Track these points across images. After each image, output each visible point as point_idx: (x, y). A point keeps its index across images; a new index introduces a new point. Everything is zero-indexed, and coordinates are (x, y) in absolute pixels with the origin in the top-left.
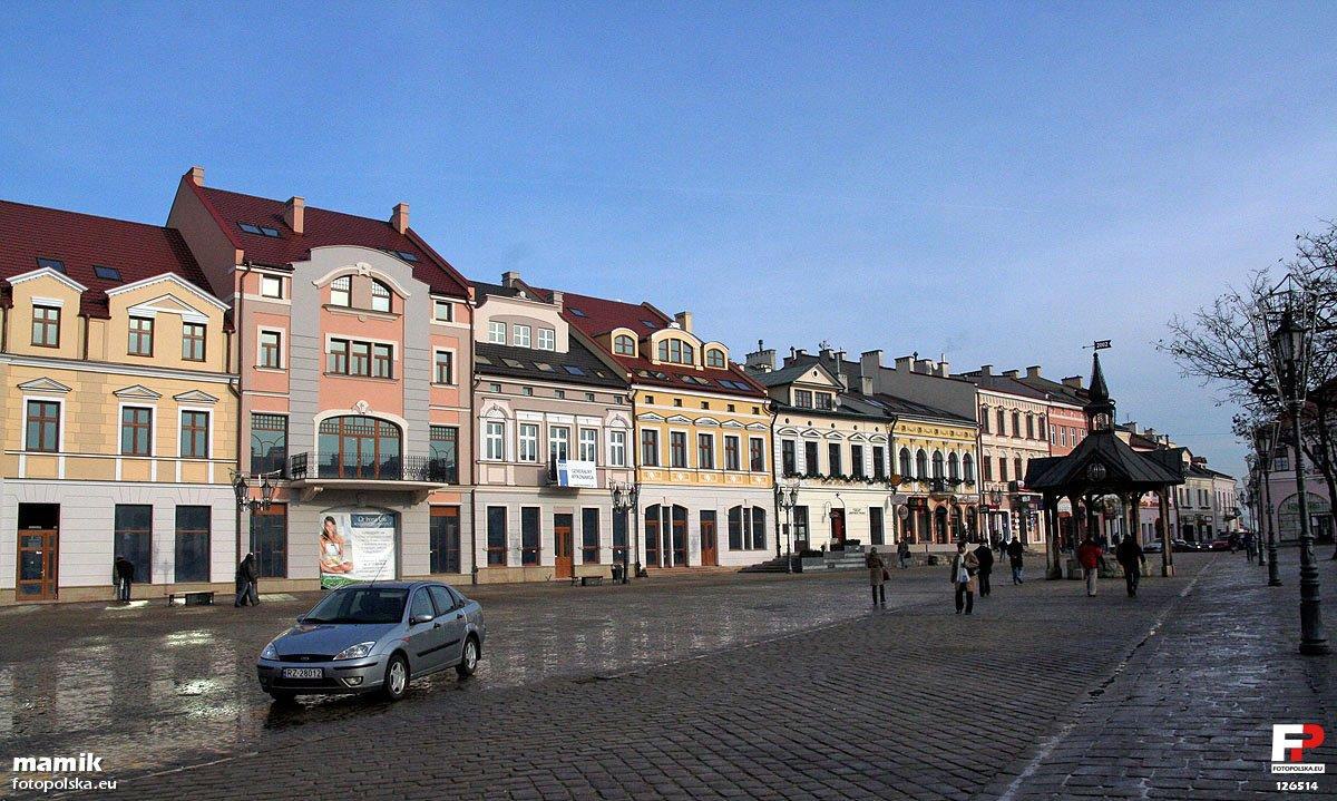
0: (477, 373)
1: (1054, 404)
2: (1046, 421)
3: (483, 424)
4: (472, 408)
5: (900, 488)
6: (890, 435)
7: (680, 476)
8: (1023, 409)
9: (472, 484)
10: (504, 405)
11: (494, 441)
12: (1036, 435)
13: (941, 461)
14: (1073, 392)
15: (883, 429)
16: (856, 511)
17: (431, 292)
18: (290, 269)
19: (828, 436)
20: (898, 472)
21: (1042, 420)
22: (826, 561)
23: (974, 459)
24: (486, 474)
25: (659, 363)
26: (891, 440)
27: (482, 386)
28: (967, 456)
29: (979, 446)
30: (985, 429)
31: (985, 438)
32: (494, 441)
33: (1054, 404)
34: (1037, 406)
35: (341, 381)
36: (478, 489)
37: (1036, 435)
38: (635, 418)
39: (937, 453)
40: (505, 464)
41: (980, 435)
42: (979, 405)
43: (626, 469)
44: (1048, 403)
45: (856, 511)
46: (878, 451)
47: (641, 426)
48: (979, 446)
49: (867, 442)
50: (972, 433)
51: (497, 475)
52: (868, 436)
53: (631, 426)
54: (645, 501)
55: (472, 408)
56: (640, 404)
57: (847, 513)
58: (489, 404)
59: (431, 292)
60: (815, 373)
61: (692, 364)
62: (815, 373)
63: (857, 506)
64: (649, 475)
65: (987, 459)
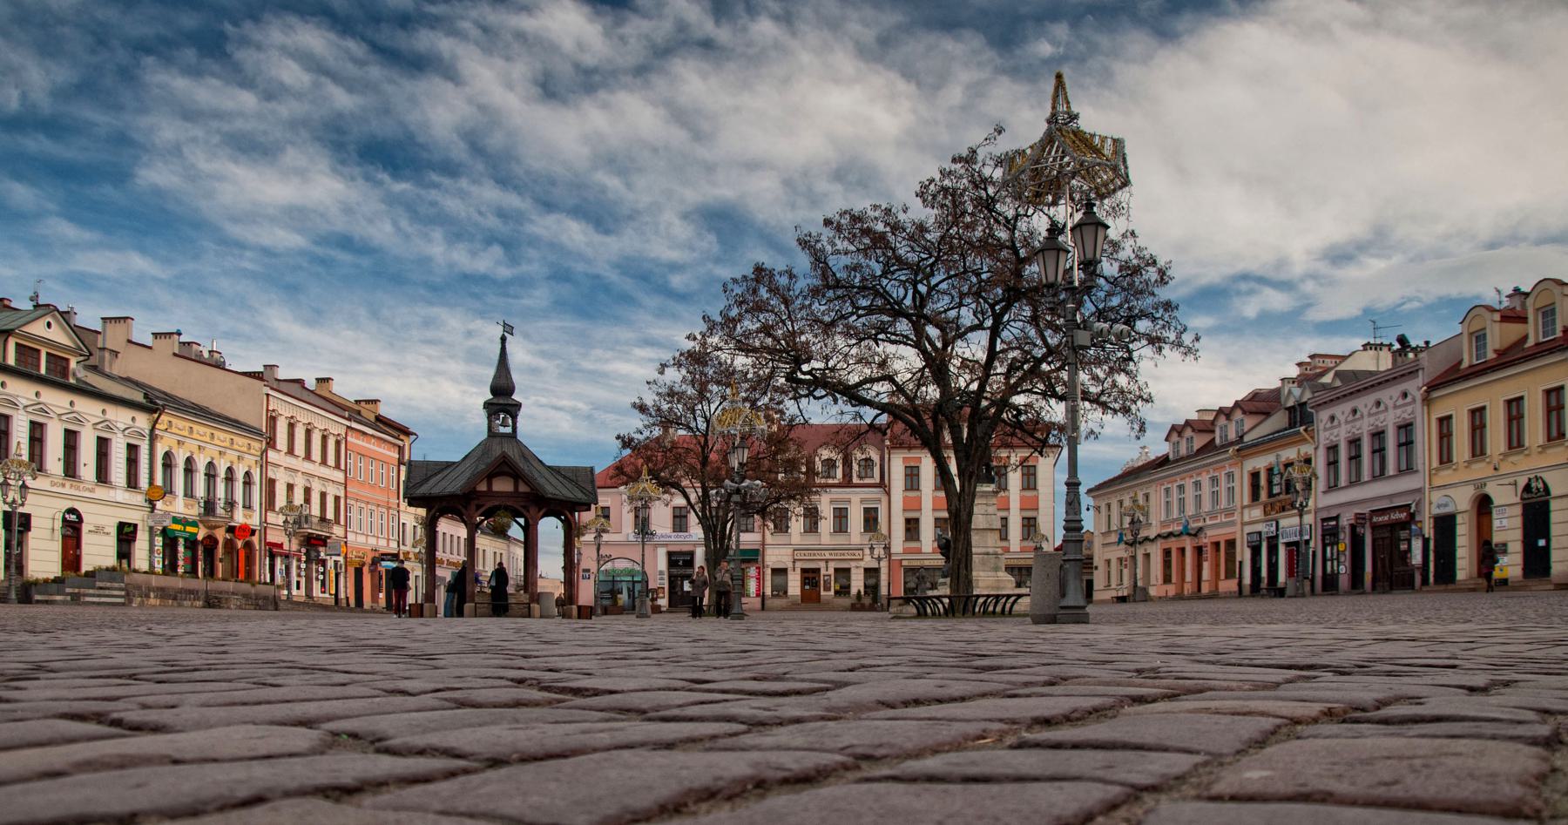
1: (354, 425)
2: (343, 446)
5: (159, 505)
8: (320, 424)
12: (331, 460)
13: (214, 476)
14: (372, 418)
15: (143, 421)
16: (98, 530)
19: (64, 418)
20: (159, 481)
21: (338, 443)
22: (68, 590)
23: (256, 477)
26: (153, 439)
28: (248, 474)
29: (264, 463)
30: (271, 443)
31: (272, 455)
33: (354, 425)
34: (336, 426)
37: (331, 460)
39: (211, 465)
41: (266, 451)
42: (267, 410)
44: (348, 423)
45: (98, 530)
46: (132, 449)
48: (264, 463)
49: (120, 435)
50: (256, 445)
52: (122, 427)
57: (85, 528)
60: (49, 325)
62: (49, 325)
63: (101, 521)
65: (271, 483)
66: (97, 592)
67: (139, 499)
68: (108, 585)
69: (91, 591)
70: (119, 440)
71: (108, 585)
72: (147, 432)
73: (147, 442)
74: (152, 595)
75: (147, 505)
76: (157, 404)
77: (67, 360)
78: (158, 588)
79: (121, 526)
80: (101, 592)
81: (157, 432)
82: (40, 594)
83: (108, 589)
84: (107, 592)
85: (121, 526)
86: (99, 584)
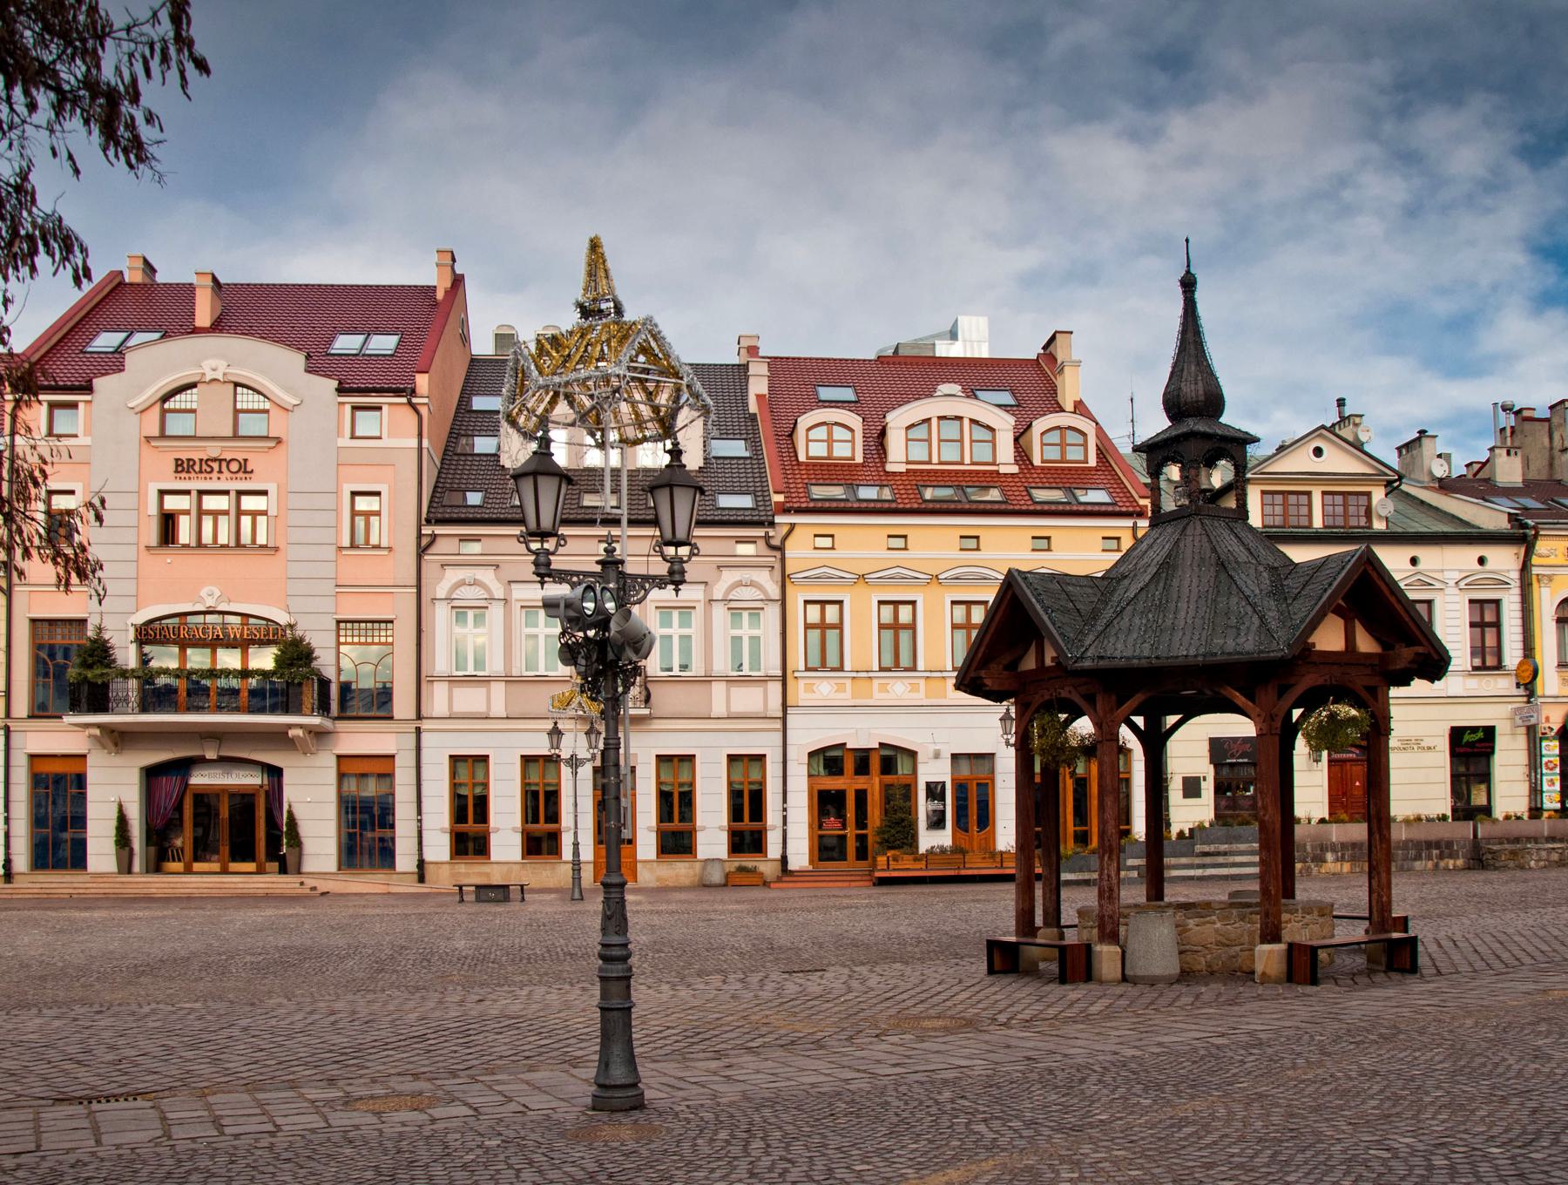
0: (428, 521)
3: (440, 616)
4: (419, 587)
6: (1525, 568)
7: (899, 688)
9: (419, 717)
10: (487, 576)
11: (676, 642)
15: (1504, 560)
17: (341, 391)
18: (87, 388)
24: (439, 700)
25: (902, 468)
27: (440, 546)
32: (676, 642)
35: (169, 557)
36: (425, 725)
38: (784, 579)
40: (485, 681)
43: (764, 680)
47: (797, 597)
51: (470, 700)
53: (775, 592)
54: (810, 734)
55: (419, 587)
56: (800, 551)
58: (453, 575)
59: (341, 391)
60: (1318, 452)
61: (994, 464)
64: (816, 690)
66: (1197, 861)
67: (1502, 684)
68: (1224, 847)
69: (1184, 860)
70: (1448, 599)
71: (1224, 847)
72: (1515, 575)
73: (1517, 591)
74: (1329, 856)
75: (1521, 691)
76: (1525, 526)
77: (1369, 494)
78: (1344, 846)
79: (1457, 734)
80: (1208, 860)
81: (1535, 571)
82: (1072, 871)
83: (1225, 854)
84: (1221, 860)
85: (1457, 734)
86: (1199, 848)
